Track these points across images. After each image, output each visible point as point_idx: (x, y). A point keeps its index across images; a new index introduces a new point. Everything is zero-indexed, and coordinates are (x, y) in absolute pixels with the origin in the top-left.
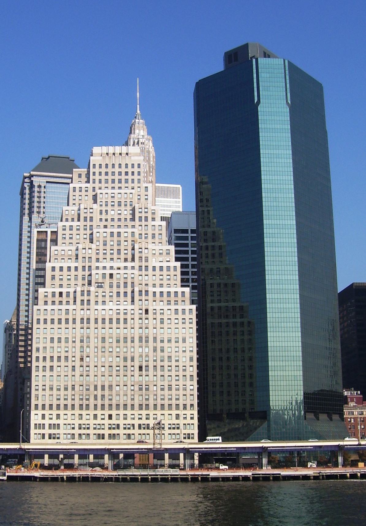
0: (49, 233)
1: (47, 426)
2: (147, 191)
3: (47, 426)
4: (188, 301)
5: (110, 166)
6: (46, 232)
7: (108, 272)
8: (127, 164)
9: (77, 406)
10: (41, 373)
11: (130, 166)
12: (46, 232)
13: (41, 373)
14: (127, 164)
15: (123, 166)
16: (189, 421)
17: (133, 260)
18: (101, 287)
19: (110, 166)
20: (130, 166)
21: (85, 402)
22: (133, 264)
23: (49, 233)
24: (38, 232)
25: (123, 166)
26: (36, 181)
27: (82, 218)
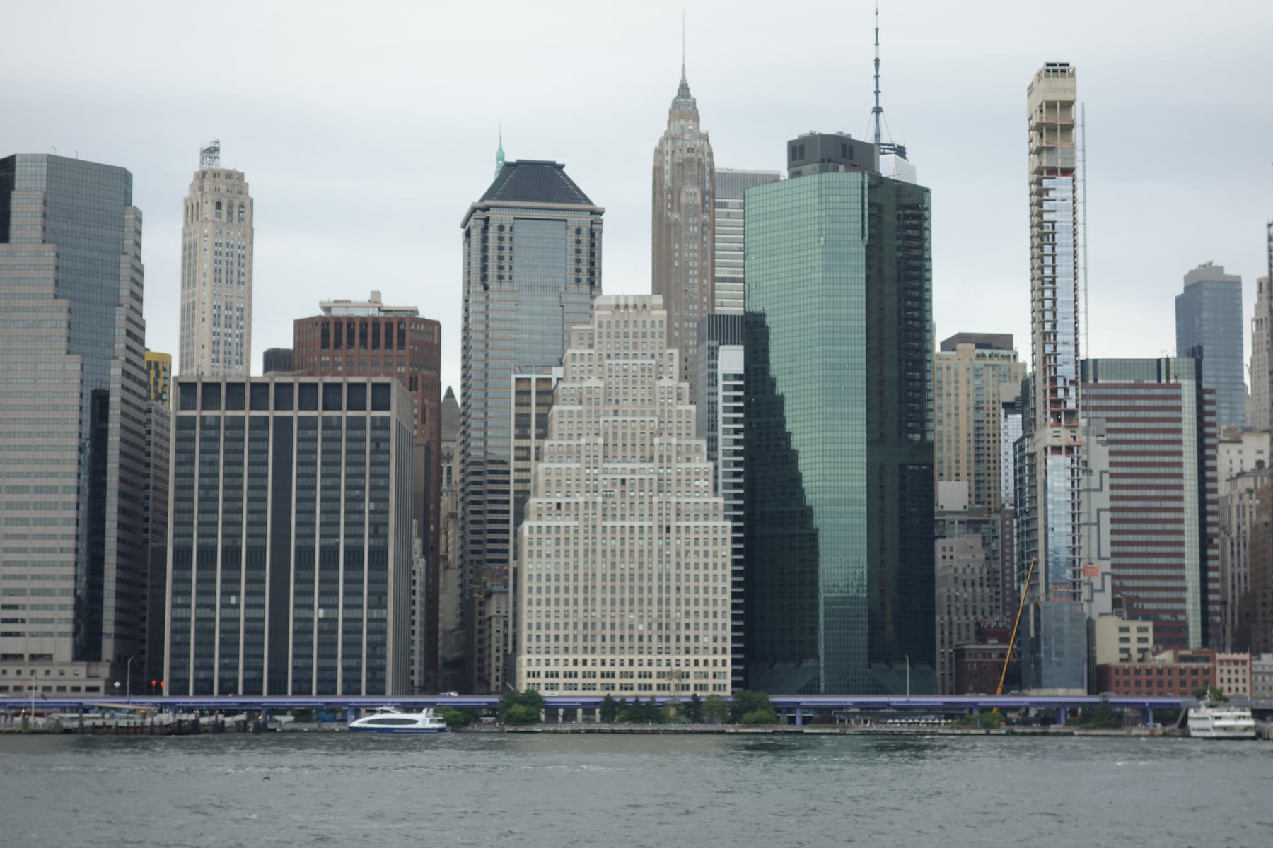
0: (534, 381)
1: (543, 675)
2: (671, 359)
3: (543, 675)
4: (721, 516)
5: (622, 325)
6: (529, 380)
7: (620, 477)
8: (644, 322)
9: (580, 649)
10: (534, 608)
11: (649, 325)
12: (529, 380)
13: (534, 608)
14: (644, 322)
15: (640, 324)
16: (719, 668)
17: (652, 459)
18: (611, 496)
19: (622, 325)
20: (649, 325)
21: (590, 644)
22: (651, 465)
23: (534, 381)
24: (517, 380)
25: (640, 324)
26: (494, 216)
27: (585, 401)
